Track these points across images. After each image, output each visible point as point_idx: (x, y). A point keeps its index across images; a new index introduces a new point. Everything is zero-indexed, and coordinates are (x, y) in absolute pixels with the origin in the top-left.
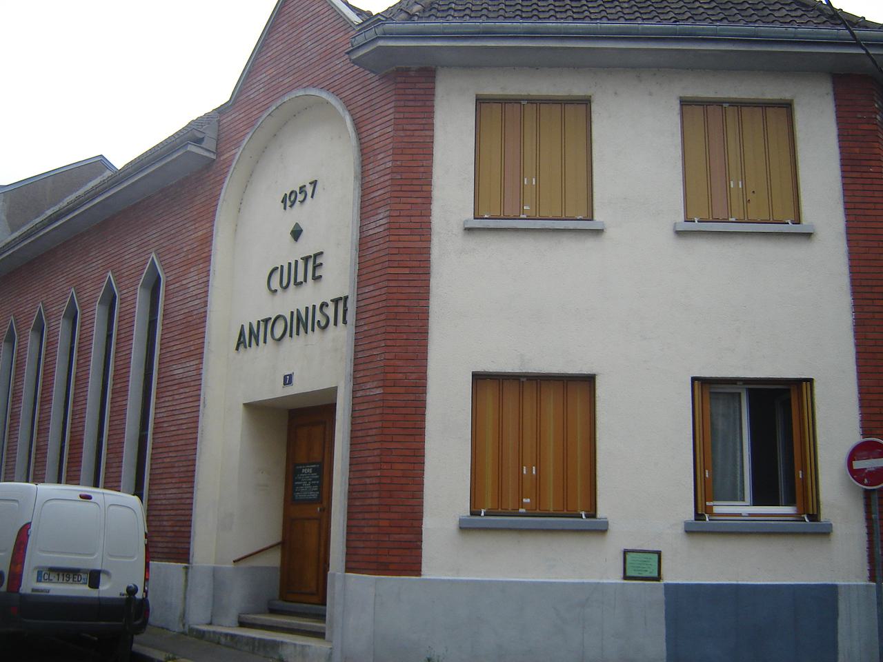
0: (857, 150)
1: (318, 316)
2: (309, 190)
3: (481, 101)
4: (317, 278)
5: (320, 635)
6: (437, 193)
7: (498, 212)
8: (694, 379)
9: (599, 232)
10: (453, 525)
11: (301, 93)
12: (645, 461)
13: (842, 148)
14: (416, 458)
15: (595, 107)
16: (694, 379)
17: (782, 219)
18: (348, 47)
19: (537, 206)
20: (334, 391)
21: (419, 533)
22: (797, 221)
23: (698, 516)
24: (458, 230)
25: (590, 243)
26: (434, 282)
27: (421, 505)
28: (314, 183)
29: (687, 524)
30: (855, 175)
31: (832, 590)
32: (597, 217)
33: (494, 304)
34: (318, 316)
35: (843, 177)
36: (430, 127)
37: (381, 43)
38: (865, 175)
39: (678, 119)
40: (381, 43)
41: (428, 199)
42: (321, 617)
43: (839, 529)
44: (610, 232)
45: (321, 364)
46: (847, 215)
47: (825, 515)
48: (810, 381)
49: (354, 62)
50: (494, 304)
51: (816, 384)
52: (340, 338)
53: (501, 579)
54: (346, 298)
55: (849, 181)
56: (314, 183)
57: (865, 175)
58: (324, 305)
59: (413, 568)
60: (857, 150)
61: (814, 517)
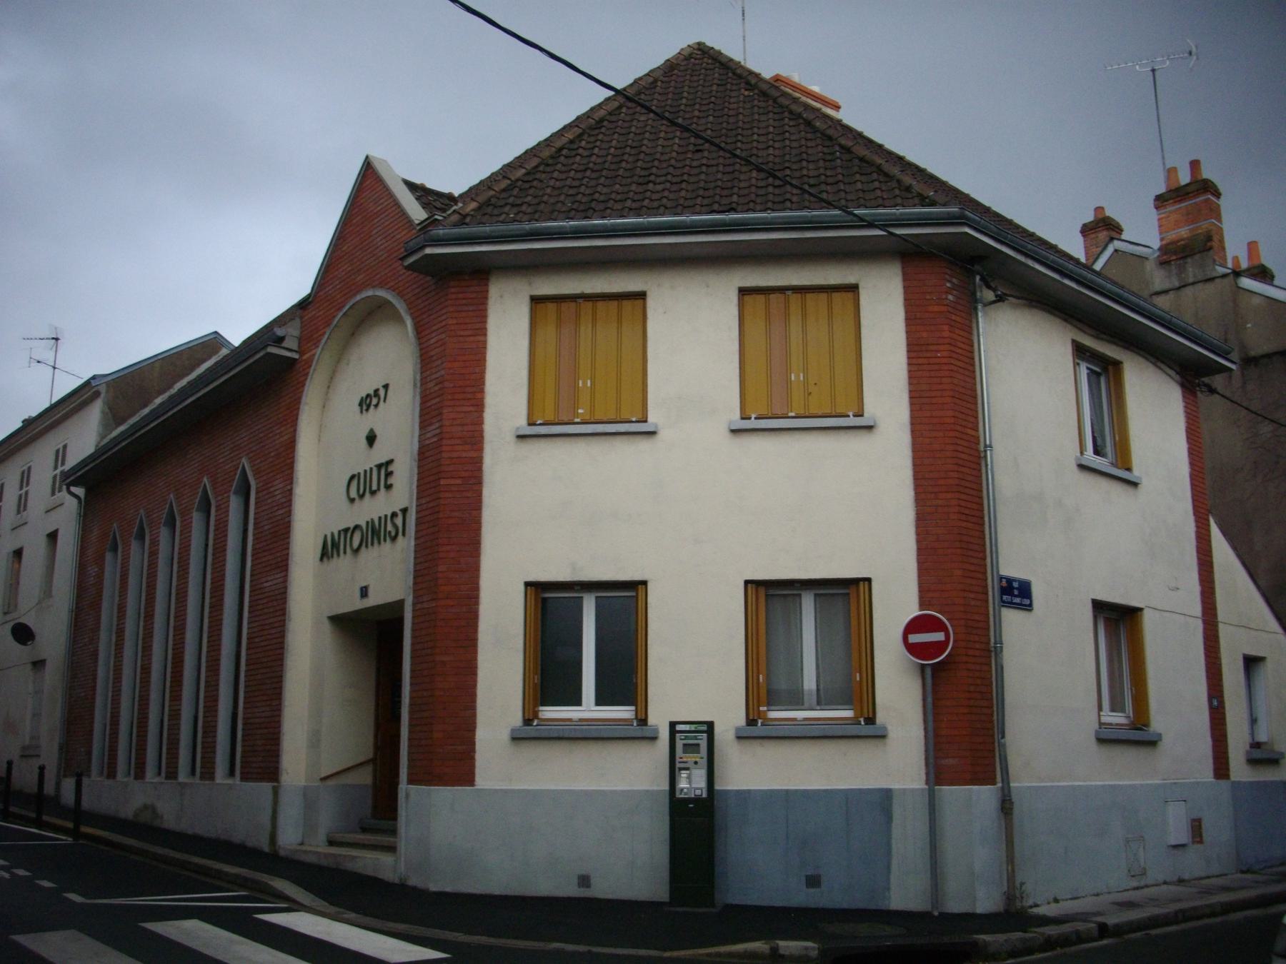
0: (925, 335)
1: (390, 527)
2: (382, 393)
3: (536, 300)
4: (389, 487)
5: (392, 849)
6: (490, 400)
7: (551, 419)
8: (747, 582)
9: (653, 433)
10: (505, 735)
11: (370, 293)
12: (695, 668)
13: (909, 333)
14: (469, 669)
15: (651, 302)
16: (747, 582)
17: (843, 413)
18: (402, 253)
19: (592, 409)
20: (400, 604)
21: (472, 743)
22: (860, 414)
23: (751, 722)
24: (510, 438)
25: (643, 445)
26: (486, 492)
27: (474, 715)
28: (386, 387)
29: (738, 729)
30: (920, 361)
31: (887, 794)
32: (651, 419)
33: (548, 511)
34: (390, 527)
35: (909, 364)
36: (483, 332)
37: (428, 251)
38: (932, 361)
39: (735, 311)
40: (428, 251)
41: (479, 406)
42: (393, 832)
43: (894, 733)
44: (664, 434)
45: (387, 575)
46: (912, 404)
47: (881, 717)
48: (869, 580)
49: (409, 268)
50: (548, 511)
51: (874, 585)
52: (405, 547)
53: (553, 787)
54: (404, 511)
55: (915, 368)
56: (386, 387)
57: (932, 361)
58: (394, 515)
59: (465, 776)
60: (925, 335)
61: (871, 720)
